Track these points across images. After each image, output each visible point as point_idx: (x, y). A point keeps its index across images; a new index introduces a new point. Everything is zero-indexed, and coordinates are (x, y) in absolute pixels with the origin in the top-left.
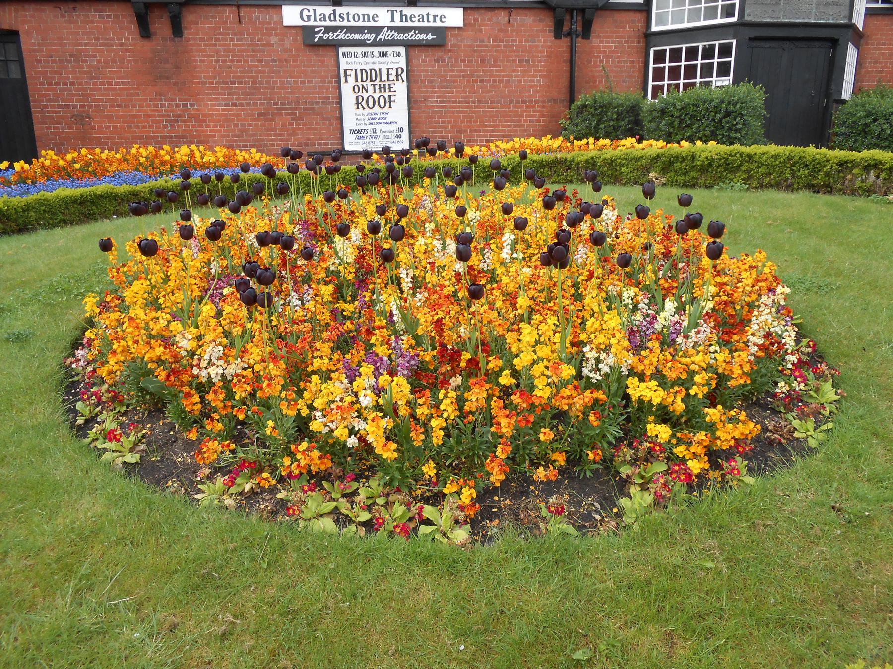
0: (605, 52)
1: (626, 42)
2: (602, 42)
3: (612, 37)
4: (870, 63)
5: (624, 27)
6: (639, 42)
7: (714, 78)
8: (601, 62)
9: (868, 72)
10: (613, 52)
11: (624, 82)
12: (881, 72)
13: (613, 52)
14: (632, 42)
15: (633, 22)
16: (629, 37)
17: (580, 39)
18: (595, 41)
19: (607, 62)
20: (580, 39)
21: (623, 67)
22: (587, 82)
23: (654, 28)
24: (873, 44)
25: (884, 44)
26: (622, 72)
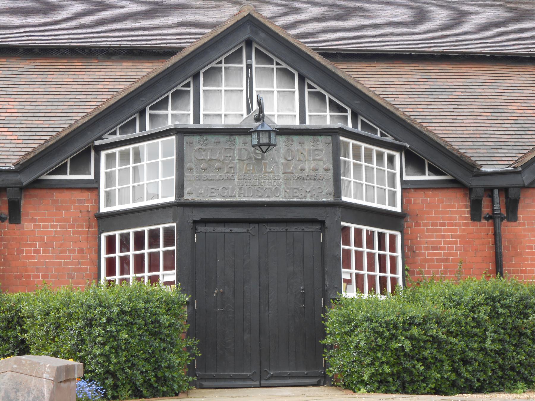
0: (42, 239)
1: (72, 226)
2: (36, 226)
3: (51, 220)
4: (427, 249)
5: (68, 208)
6: (89, 226)
7: (161, 272)
8: (37, 252)
9: (426, 261)
10: (54, 239)
11: (70, 276)
12: (447, 260)
13: (54, 239)
14: (82, 226)
15: (81, 202)
16: (75, 220)
17: (6, 224)
18: (27, 226)
19: (45, 251)
20: (6, 224)
21: (69, 257)
22: (20, 277)
23: (104, 209)
24: (426, 225)
25: (443, 225)
26: (66, 263)
